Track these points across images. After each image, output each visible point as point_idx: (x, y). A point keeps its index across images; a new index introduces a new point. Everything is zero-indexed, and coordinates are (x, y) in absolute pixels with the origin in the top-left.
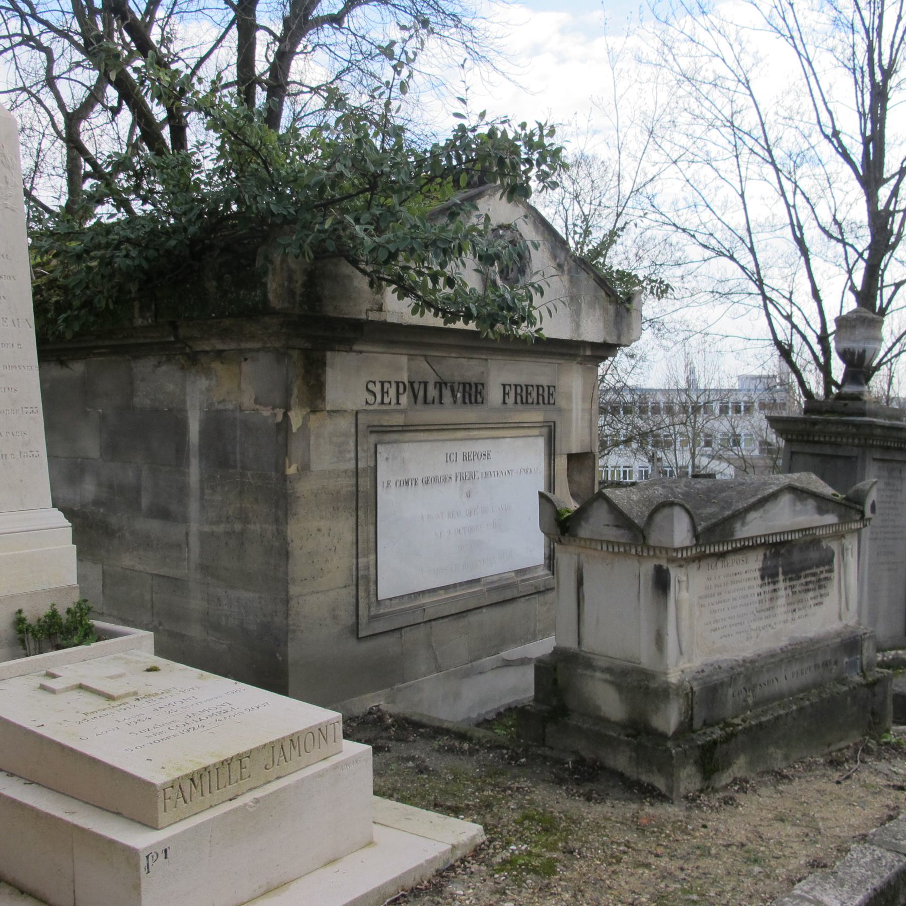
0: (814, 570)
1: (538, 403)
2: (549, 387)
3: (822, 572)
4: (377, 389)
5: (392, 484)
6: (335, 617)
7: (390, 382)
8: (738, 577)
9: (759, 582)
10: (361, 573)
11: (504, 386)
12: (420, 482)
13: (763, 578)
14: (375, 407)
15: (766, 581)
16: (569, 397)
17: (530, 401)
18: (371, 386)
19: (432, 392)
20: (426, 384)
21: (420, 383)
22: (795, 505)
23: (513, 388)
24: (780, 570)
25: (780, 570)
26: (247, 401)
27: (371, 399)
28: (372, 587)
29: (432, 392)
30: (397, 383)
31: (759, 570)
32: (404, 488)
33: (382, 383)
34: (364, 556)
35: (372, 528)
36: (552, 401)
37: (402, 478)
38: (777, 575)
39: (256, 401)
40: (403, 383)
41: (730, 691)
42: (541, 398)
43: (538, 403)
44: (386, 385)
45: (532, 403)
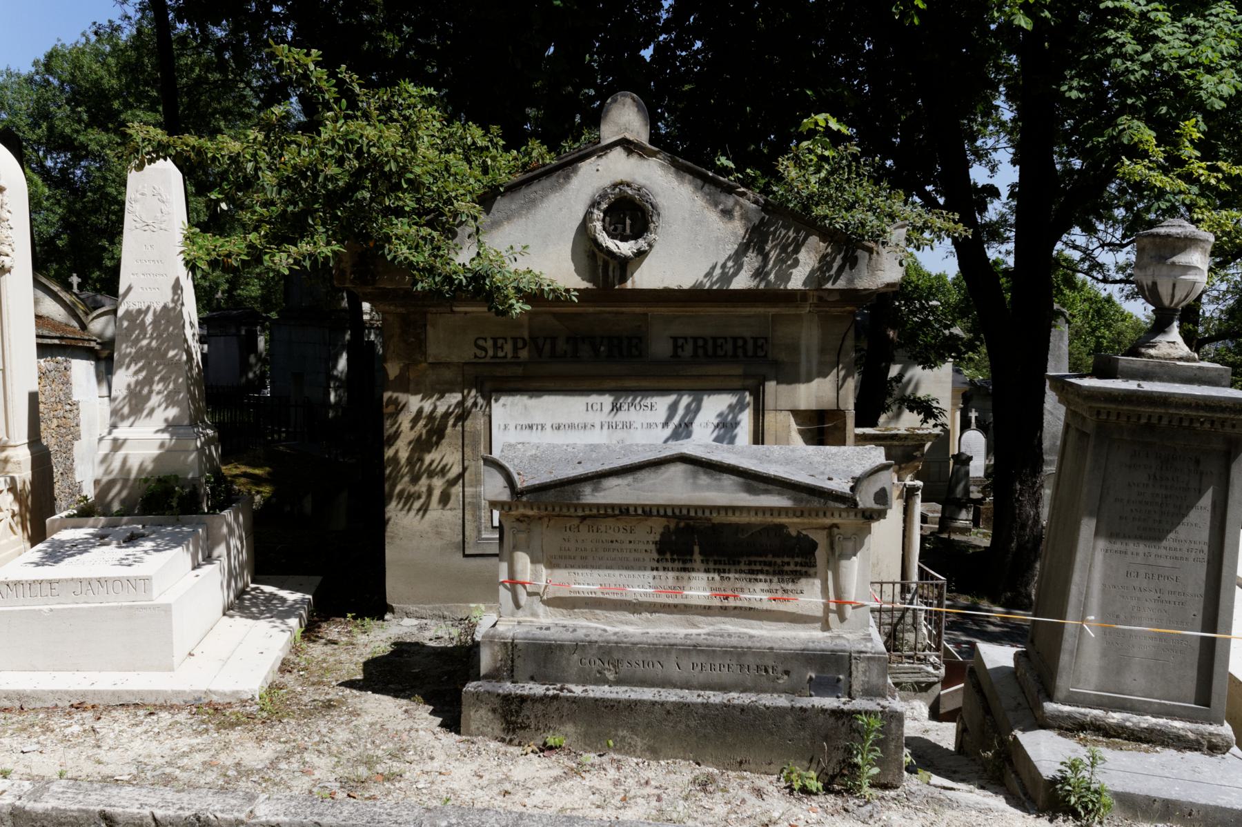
0: (770, 558)
1: (735, 355)
2: (755, 339)
3: (788, 564)
5: (512, 427)
6: (438, 533)
7: (505, 339)
8: (615, 545)
9: (656, 556)
10: (467, 500)
11: (675, 339)
12: (548, 427)
13: (661, 551)
14: (487, 360)
15: (668, 556)
16: (794, 349)
17: (720, 353)
18: (481, 342)
19: (561, 346)
20: (554, 339)
21: (545, 338)
22: (695, 477)
23: (691, 342)
24: (696, 549)
25: (696, 549)
27: (480, 353)
29: (561, 346)
30: (515, 340)
31: (656, 543)
32: (527, 432)
33: (495, 340)
37: (526, 422)
38: (692, 553)
40: (523, 339)
41: (576, 657)
43: (735, 355)
44: (500, 342)
45: (725, 355)
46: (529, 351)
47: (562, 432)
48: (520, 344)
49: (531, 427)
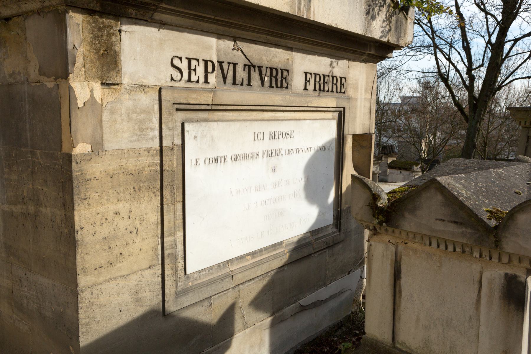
1: (332, 91)
2: (341, 78)
4: (184, 65)
5: (201, 162)
7: (198, 60)
10: (167, 252)
11: (306, 73)
12: (229, 159)
14: (182, 84)
16: (356, 89)
18: (176, 62)
19: (241, 74)
20: (235, 65)
21: (229, 63)
23: (313, 76)
26: (34, 73)
27: (176, 75)
28: (181, 262)
29: (241, 74)
30: (206, 62)
32: (214, 165)
33: (189, 60)
34: (170, 235)
35: (179, 206)
36: (343, 91)
37: (212, 156)
39: (41, 72)
42: (335, 87)
44: (194, 63)
45: (328, 91)
46: (217, 77)
47: (238, 162)
48: (210, 69)
49: (216, 160)
